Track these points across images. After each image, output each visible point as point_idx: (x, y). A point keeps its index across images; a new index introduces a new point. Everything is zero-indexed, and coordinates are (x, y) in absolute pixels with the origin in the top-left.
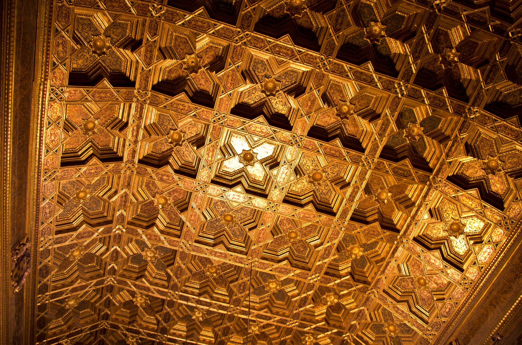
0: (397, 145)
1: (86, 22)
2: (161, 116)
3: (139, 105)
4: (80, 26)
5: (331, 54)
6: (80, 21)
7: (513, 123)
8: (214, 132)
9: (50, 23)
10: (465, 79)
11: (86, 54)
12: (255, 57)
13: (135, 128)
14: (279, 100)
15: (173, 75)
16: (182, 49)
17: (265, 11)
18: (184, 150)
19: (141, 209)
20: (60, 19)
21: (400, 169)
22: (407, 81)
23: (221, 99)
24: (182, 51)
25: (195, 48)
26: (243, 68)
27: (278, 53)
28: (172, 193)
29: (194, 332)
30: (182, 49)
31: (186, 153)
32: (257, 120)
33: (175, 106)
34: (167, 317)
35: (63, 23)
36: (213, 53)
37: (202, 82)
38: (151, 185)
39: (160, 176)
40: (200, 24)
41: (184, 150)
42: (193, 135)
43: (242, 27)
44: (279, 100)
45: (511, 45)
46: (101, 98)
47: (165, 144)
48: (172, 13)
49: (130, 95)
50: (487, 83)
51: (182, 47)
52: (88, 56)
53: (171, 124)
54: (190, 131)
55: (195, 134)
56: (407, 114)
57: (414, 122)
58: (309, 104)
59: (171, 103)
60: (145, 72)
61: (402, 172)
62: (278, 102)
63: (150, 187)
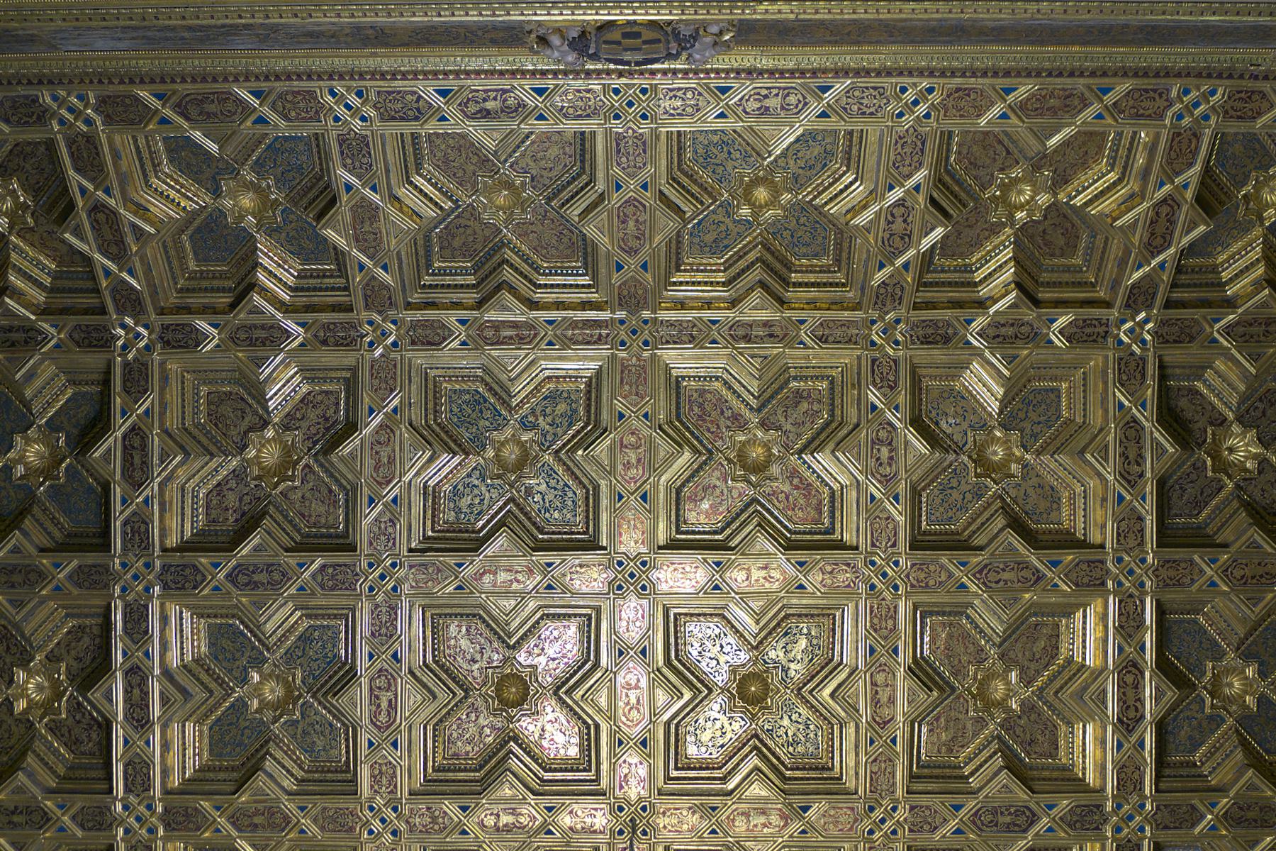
2: (1052, 396)
3: (1101, 330)
8: (1085, 567)
11: (1256, 161)
13: (1025, 329)
14: (1205, 724)
15: (1183, 403)
16: (1264, 413)
18: (964, 487)
19: (702, 392)
23: (1192, 562)
24: (1258, 414)
28: (796, 481)
29: (199, 695)
30: (1264, 413)
31: (955, 494)
32: (1163, 686)
34: (261, 577)
38: (805, 406)
39: (883, 434)
41: (964, 487)
42: (1021, 502)
44: (1205, 724)
46: (1152, 222)
47: (965, 425)
49: (1141, 299)
51: (1269, 412)
53: (1037, 429)
54: (1030, 491)
55: (1028, 507)
58: (1250, 815)
59: (1135, 421)
60: (1208, 329)
62: (1194, 722)
63: (797, 405)
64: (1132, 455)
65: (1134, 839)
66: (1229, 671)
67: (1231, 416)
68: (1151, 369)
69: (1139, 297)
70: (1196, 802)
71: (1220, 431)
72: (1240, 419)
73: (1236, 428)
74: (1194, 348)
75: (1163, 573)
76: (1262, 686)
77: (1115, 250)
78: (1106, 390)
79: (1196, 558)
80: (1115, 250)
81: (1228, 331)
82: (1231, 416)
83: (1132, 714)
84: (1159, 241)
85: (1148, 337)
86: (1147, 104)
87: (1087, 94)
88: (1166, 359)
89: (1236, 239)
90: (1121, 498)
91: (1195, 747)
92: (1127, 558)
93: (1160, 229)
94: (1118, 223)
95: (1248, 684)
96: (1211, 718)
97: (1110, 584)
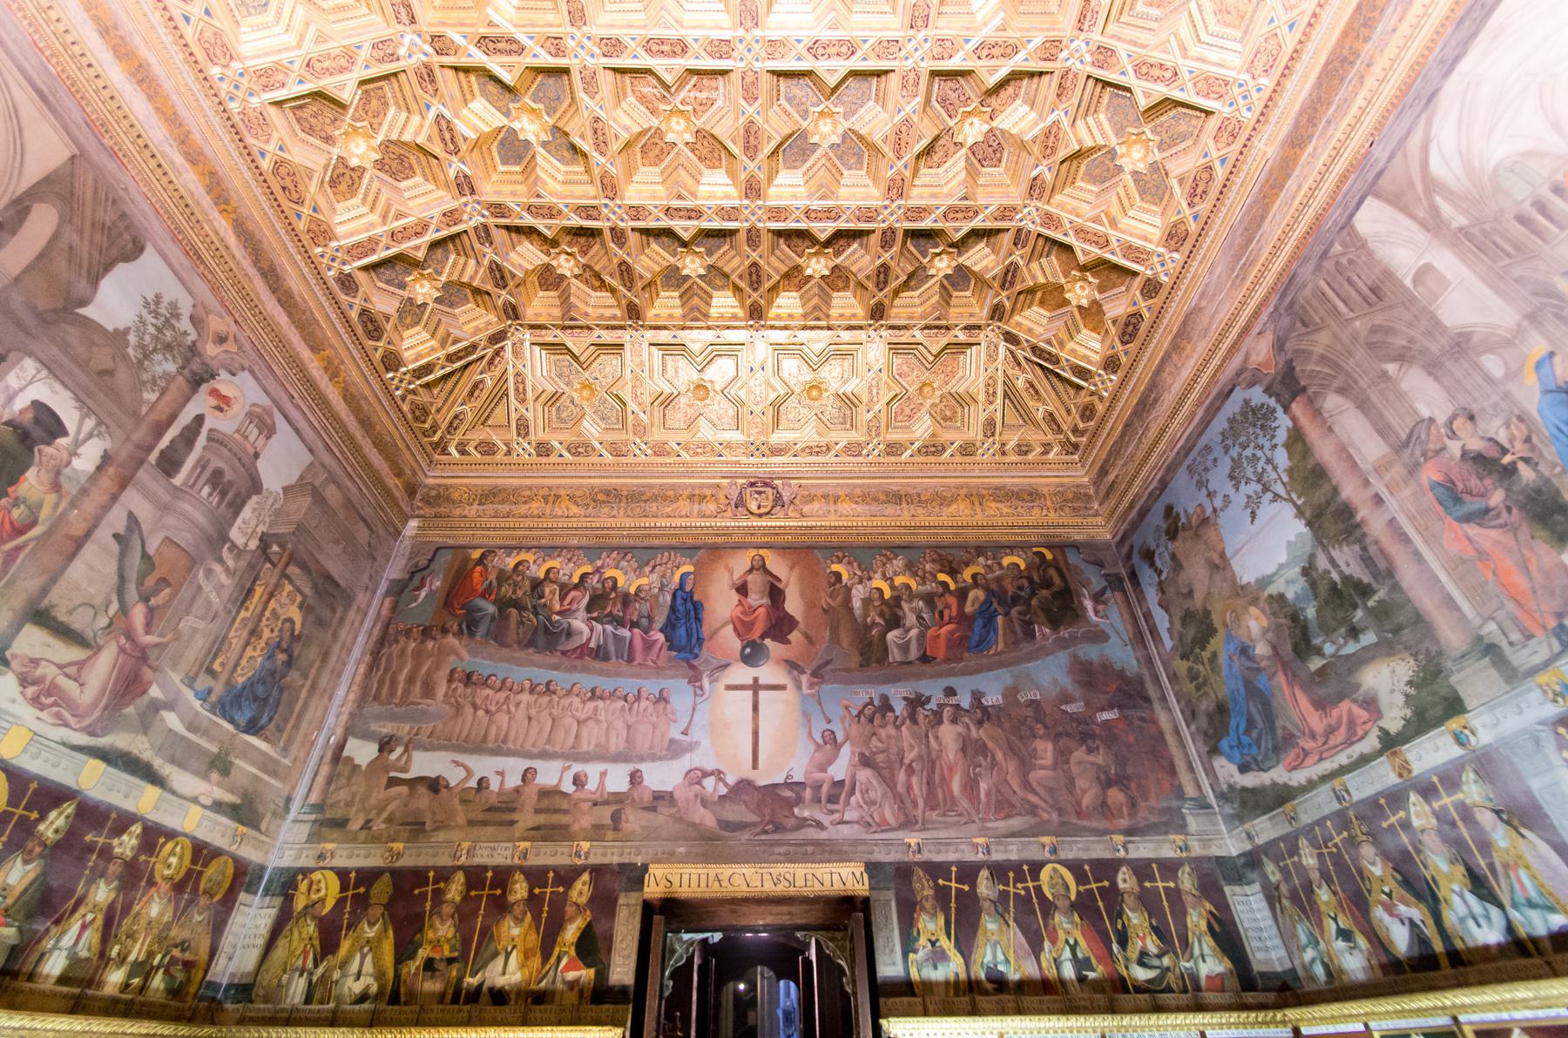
0: (542, 84)
3: (1085, 27)
5: (749, 231)
7: (417, 248)
10: (520, 242)
12: (863, 172)
17: (861, 245)
21: (509, 53)
22: (612, 229)
25: (967, 159)
26: (883, 163)
27: (829, 211)
33: (1009, 50)
36: (935, 158)
37: (954, 95)
40: (960, 215)
43: (893, 231)
45: (508, 318)
48: (1003, 218)
50: (492, 262)
52: (1165, 136)
56: (566, 154)
57: (544, 144)
61: (499, 46)
64: (993, 51)
65: (735, 54)
66: (835, 124)
67: (994, 124)
68: (1047, 66)
69: (1104, 54)
70: (759, 101)
71: (987, 116)
72: (991, 130)
73: (986, 128)
74: (1052, 96)
75: (912, 76)
76: (825, 145)
77: (1144, 37)
78: (1042, 30)
79: (918, 99)
80: (1144, 37)
81: (1056, 123)
82: (994, 124)
83: (821, 51)
84: (1144, 69)
85: (1069, 63)
86: (1264, 59)
87: (1296, 12)
88: (1046, 78)
89: (1113, 127)
90: (967, 41)
91: (788, 100)
92: (927, 45)
93: (1156, 72)
94: (1172, 39)
95: (823, 137)
96: (806, 112)
97: (911, 32)
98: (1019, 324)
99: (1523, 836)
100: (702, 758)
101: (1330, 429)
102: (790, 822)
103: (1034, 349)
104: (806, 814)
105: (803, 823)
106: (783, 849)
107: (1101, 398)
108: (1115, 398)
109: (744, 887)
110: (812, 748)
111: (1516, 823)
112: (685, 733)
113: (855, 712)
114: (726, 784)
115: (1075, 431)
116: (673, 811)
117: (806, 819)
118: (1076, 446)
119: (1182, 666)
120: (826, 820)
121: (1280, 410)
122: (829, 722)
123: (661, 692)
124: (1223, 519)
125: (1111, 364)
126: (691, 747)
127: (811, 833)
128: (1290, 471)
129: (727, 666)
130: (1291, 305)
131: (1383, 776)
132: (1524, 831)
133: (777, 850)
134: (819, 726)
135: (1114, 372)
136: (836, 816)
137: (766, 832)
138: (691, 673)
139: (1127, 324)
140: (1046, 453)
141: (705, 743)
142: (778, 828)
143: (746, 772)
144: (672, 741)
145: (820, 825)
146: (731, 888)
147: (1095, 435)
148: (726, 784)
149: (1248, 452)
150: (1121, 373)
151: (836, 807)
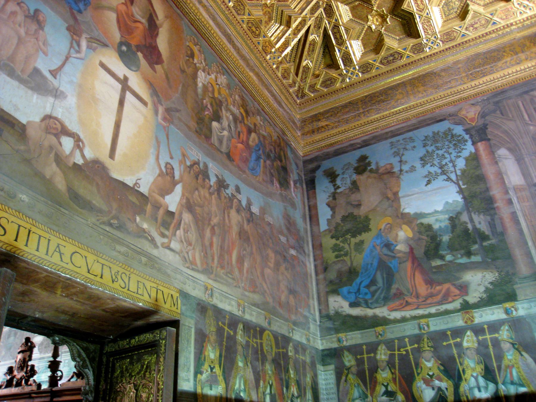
1: (446, 9)
4: (452, 11)
6: (447, 14)
9: (459, 44)
20: (453, 38)
35: (455, 34)
98: (337, 7)
99: (522, 355)
100: (67, 111)
101: (496, 163)
102: (131, 227)
103: (336, 27)
104: (145, 226)
105: (142, 234)
106: (123, 249)
107: (343, 81)
108: (351, 85)
109: (83, 271)
110: (158, 172)
111: (521, 349)
112: (54, 73)
113: (188, 164)
114: (83, 156)
115: (312, 88)
116: (22, 148)
117: (144, 230)
118: (303, 95)
119: (329, 242)
120: (159, 240)
121: (470, 143)
122: (172, 158)
123: (37, 11)
124: (405, 178)
125: (365, 67)
126: (57, 94)
127: (147, 246)
128: (463, 172)
129: (105, 45)
130: (497, 103)
131: (458, 321)
132: (524, 353)
133: (118, 247)
134: (164, 159)
135: (363, 73)
136: (166, 240)
137: (111, 225)
138: (72, 22)
139: (391, 55)
140: (291, 86)
141: (71, 100)
142: (120, 228)
143: (104, 156)
144: (36, 71)
145: (153, 241)
146: (70, 266)
147: (322, 96)
148: (83, 156)
149: (440, 152)
150: (367, 76)
151: (167, 233)
